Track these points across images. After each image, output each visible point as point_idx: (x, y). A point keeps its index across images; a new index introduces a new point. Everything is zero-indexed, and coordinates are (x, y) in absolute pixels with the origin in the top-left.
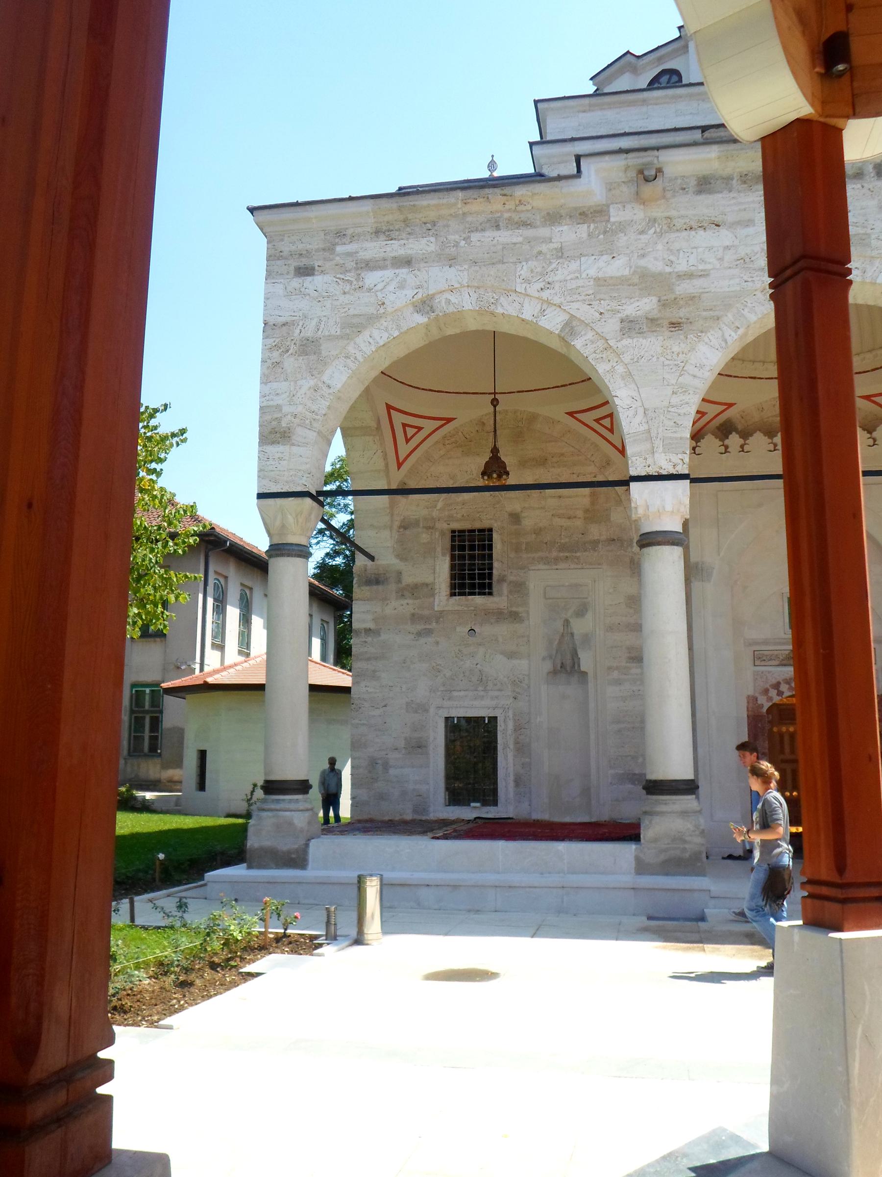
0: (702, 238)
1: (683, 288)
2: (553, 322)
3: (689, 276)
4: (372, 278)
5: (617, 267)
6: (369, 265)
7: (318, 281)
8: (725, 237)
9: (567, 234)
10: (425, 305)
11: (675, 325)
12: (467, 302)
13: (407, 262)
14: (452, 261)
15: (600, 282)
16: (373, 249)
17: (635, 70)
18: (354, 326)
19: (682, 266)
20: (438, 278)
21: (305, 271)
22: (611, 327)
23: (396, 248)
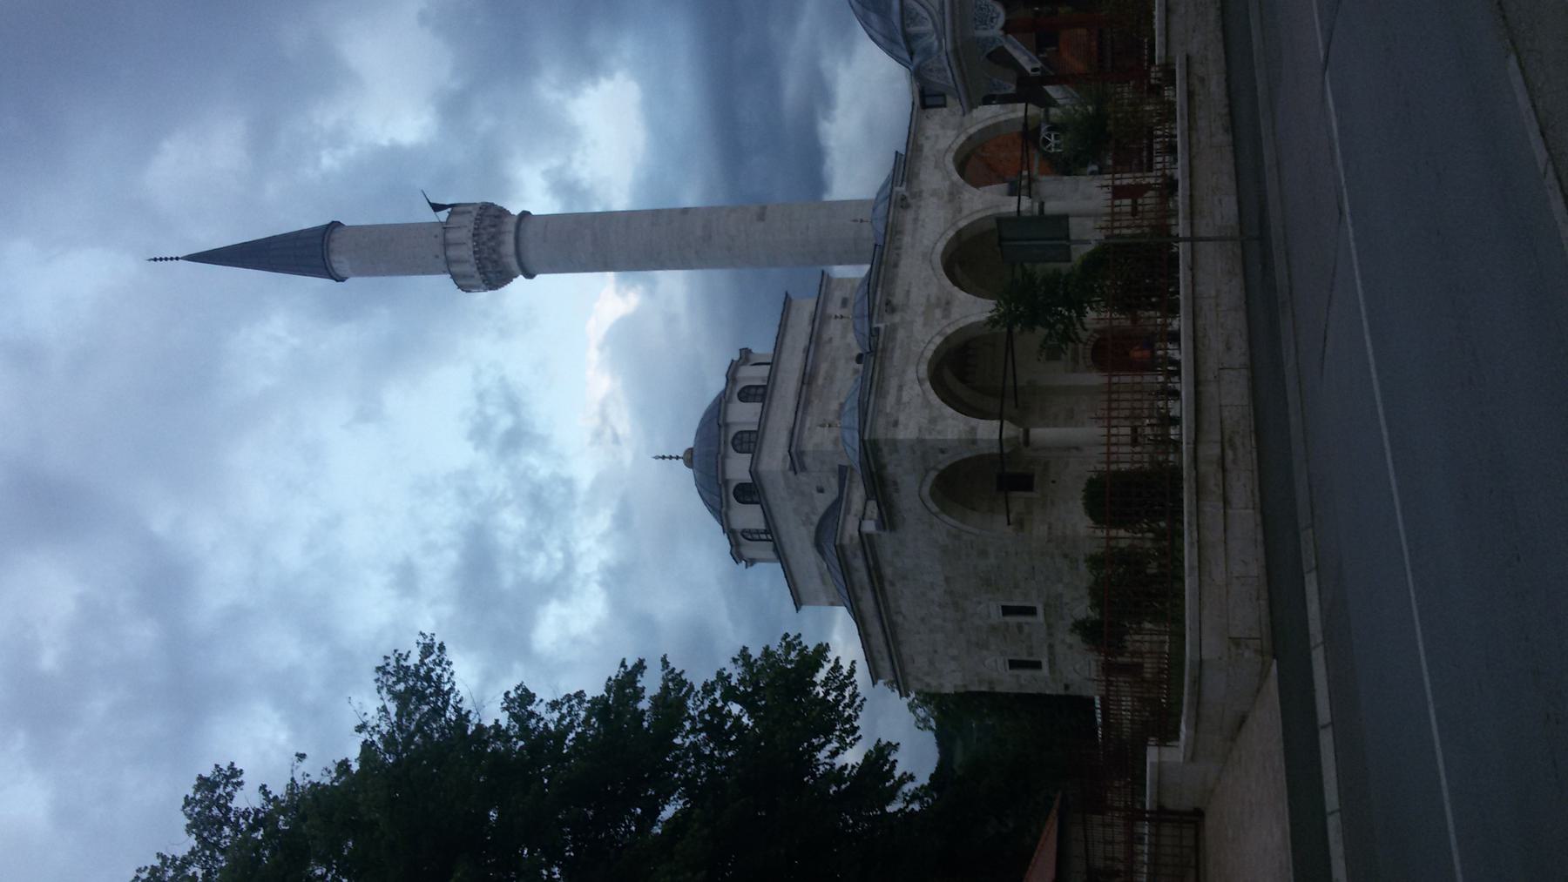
1: (933, 300)
2: (938, 340)
3: (928, 299)
4: (905, 398)
5: (919, 321)
6: (899, 401)
7: (902, 418)
9: (901, 334)
10: (920, 382)
11: (948, 303)
12: (923, 368)
13: (900, 388)
14: (904, 372)
15: (925, 325)
16: (891, 399)
17: (725, 457)
20: (911, 374)
21: (896, 424)
22: (945, 322)
23: (893, 392)
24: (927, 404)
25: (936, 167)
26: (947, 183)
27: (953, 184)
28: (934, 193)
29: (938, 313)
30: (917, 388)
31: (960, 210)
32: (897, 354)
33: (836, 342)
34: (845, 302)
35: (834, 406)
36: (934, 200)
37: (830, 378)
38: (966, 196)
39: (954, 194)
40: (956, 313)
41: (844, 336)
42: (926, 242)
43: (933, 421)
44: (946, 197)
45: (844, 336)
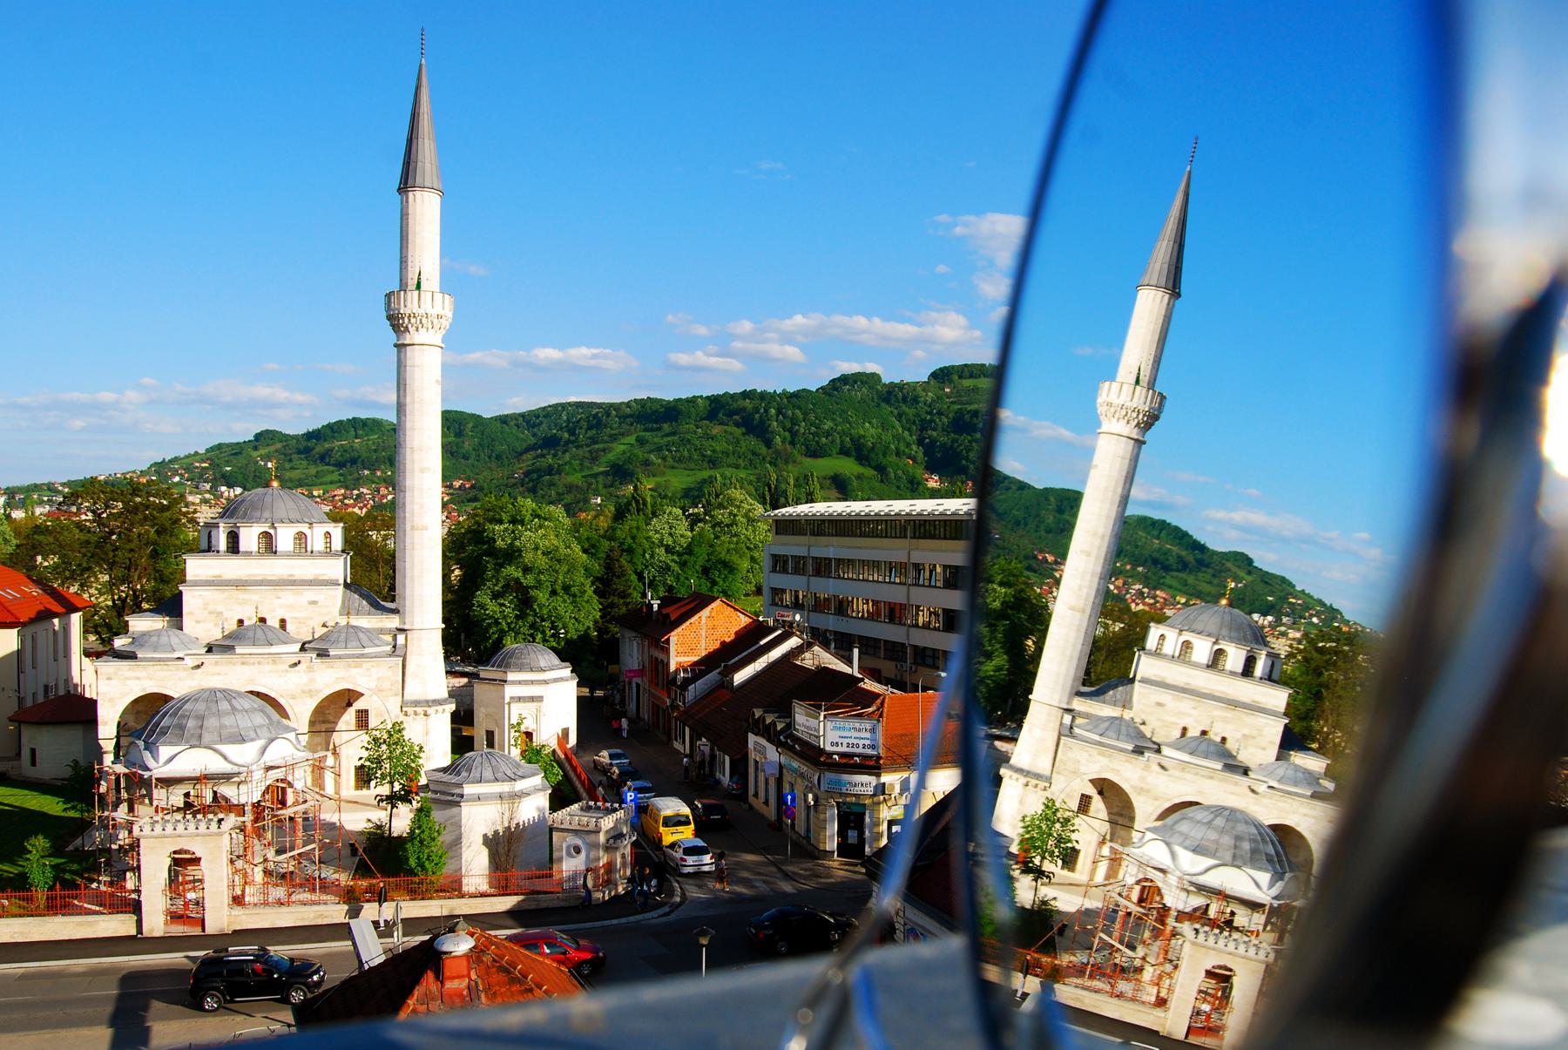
7: (113, 682)
16: (129, 674)
27: (318, 691)
31: (293, 697)
33: (278, 602)
34: (314, 603)
35: (220, 608)
37: (244, 603)
41: (281, 606)
43: (111, 700)
45: (281, 606)
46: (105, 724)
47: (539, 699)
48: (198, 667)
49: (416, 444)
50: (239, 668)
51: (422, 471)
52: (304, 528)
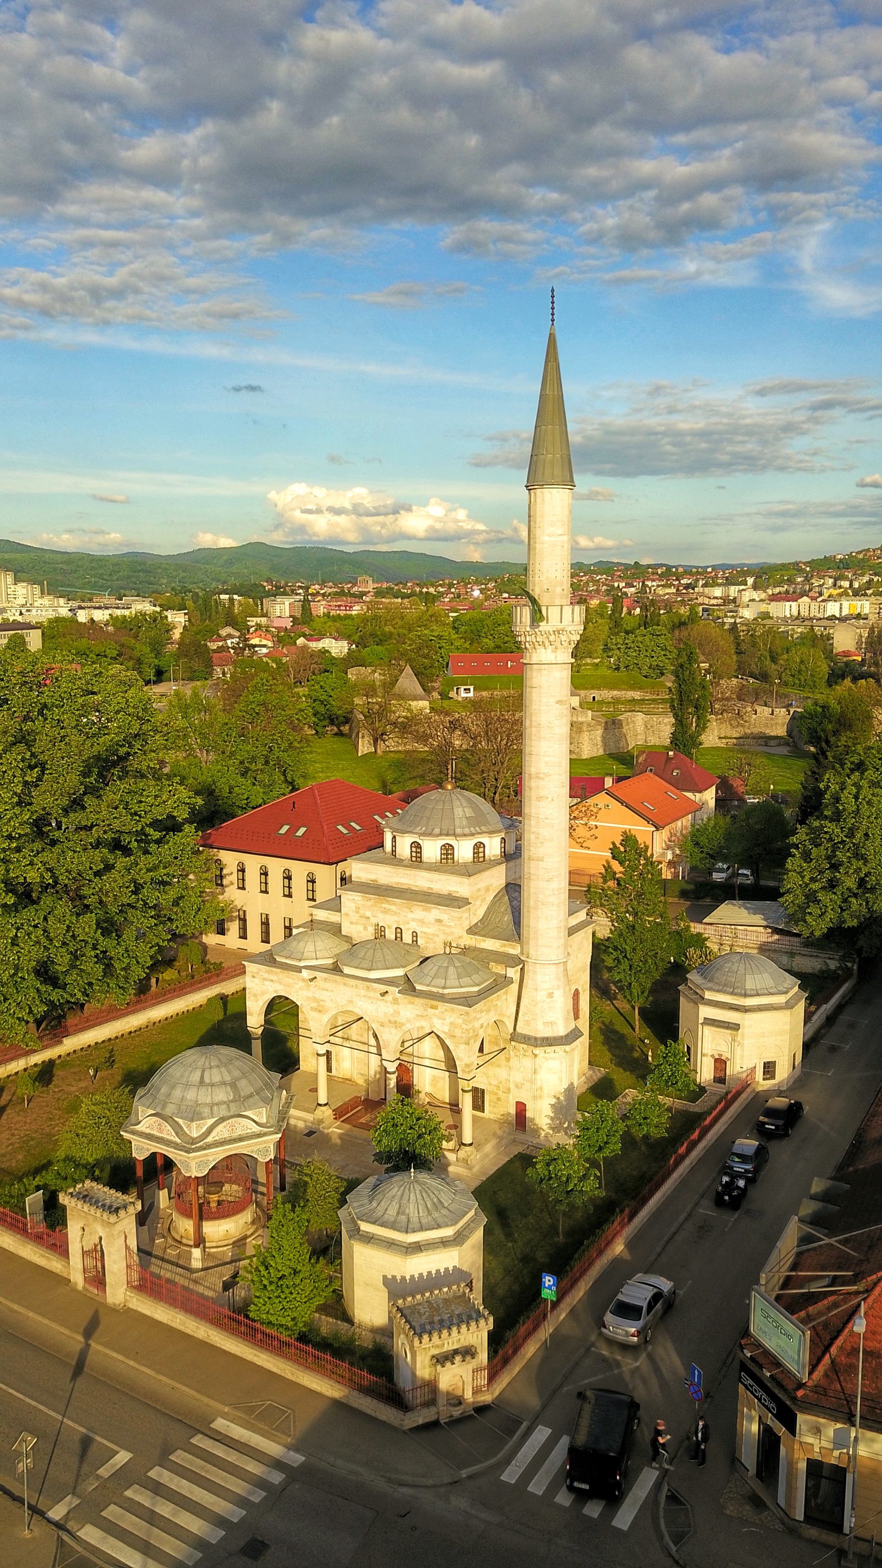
0: (325, 992)
1: (321, 1003)
4: (266, 982)
5: (310, 995)
6: (265, 979)
7: (256, 980)
8: (329, 994)
14: (280, 983)
15: (308, 997)
16: (266, 976)
18: (263, 993)
19: (321, 998)
21: (254, 977)
24: (263, 993)
25: (417, 1015)
26: (404, 1021)
27: (403, 1024)
28: (397, 1013)
29: (314, 1005)
30: (271, 989)
32: (291, 981)
33: (411, 916)
35: (368, 914)
36: (391, 1011)
37: (385, 911)
38: (394, 1031)
39: (396, 1025)
40: (315, 1014)
41: (413, 920)
42: (360, 1003)
43: (255, 995)
44: (393, 1019)
45: (413, 920)
46: (251, 1015)
47: (736, 1027)
48: (311, 980)
49: (533, 770)
50: (342, 987)
51: (539, 799)
52: (451, 841)
